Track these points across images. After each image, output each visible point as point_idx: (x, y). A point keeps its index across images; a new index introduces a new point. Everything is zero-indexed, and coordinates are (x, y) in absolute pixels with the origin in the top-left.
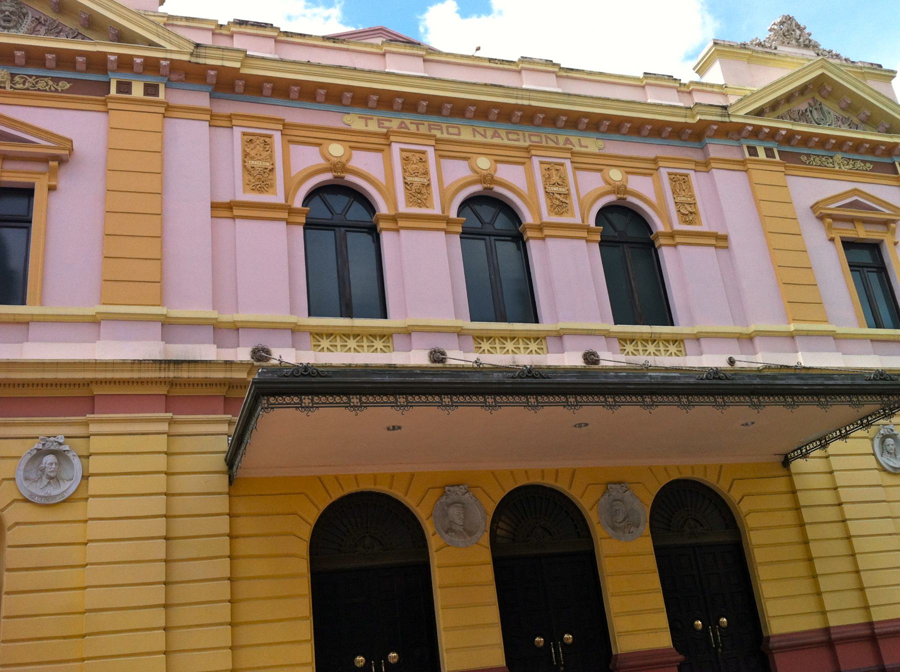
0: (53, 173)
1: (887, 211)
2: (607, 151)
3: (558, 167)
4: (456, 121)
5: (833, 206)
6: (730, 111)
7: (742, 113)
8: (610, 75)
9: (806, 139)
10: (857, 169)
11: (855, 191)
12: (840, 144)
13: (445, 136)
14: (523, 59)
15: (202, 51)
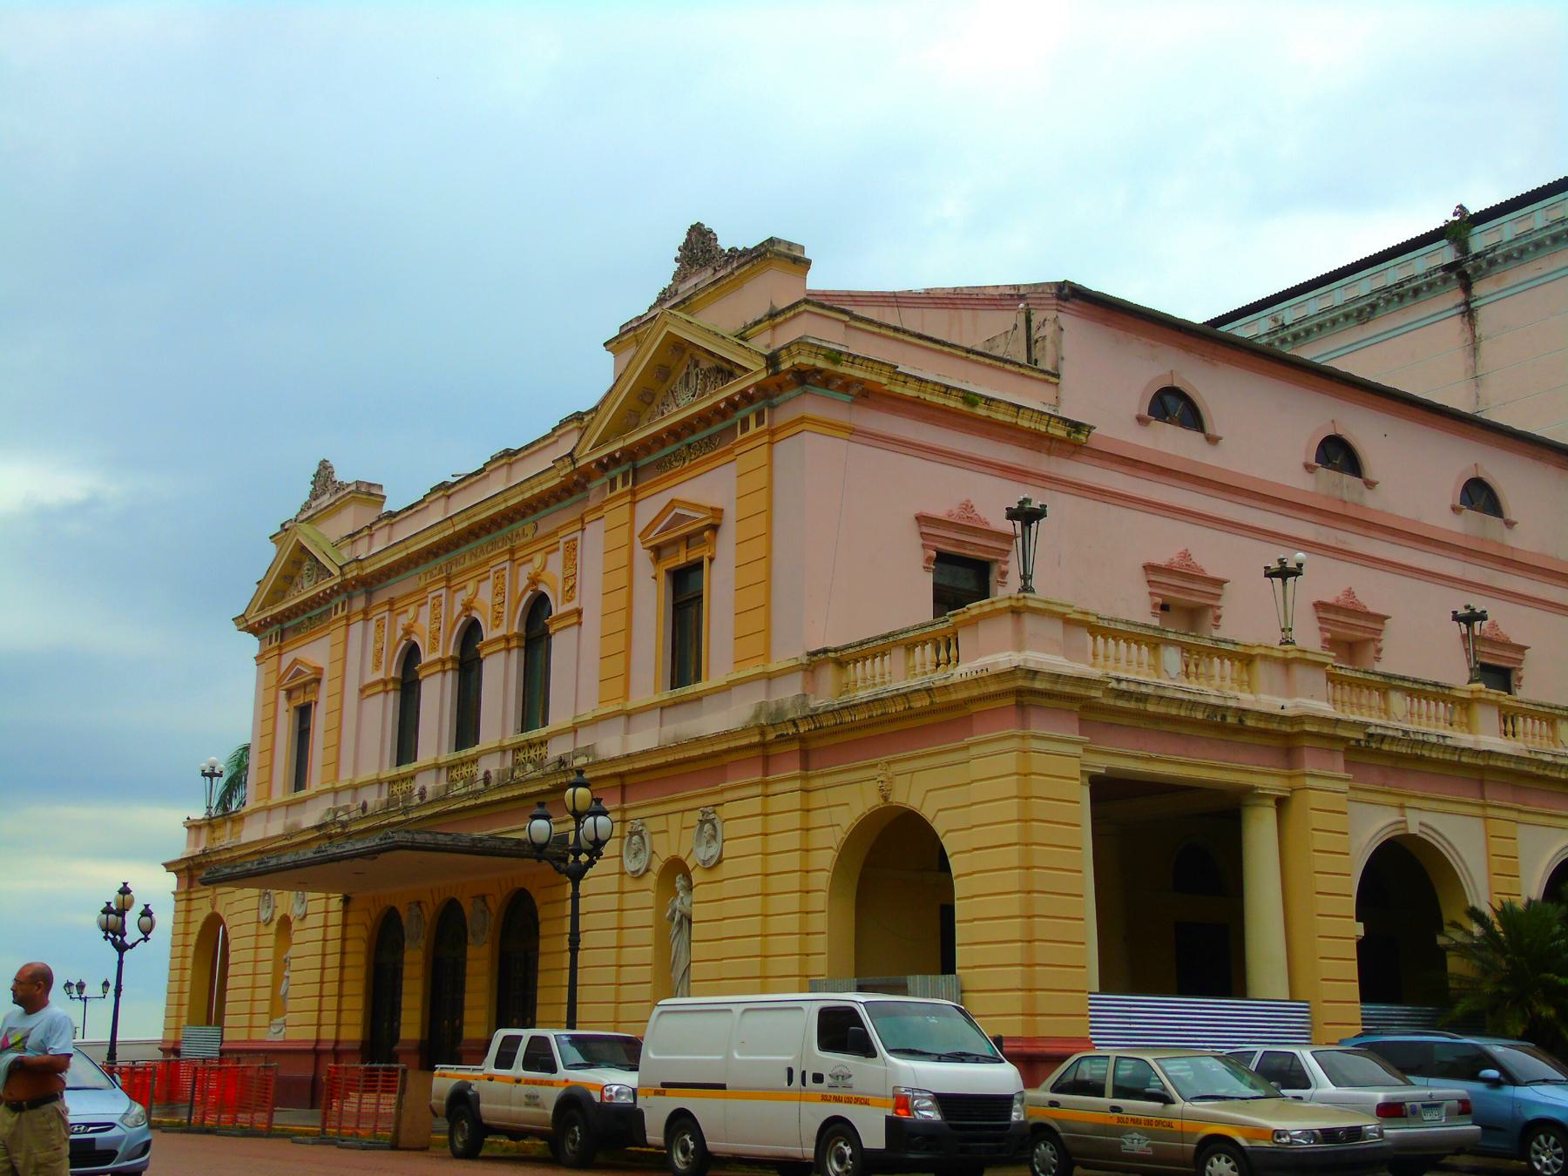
0: (316, 692)
1: (701, 516)
2: (541, 532)
3: (504, 572)
4: (463, 549)
5: (652, 536)
6: (576, 455)
7: (587, 451)
8: (538, 441)
9: (646, 446)
10: (704, 454)
11: (672, 504)
12: (675, 433)
13: (460, 568)
14: (484, 465)
15: (344, 570)
